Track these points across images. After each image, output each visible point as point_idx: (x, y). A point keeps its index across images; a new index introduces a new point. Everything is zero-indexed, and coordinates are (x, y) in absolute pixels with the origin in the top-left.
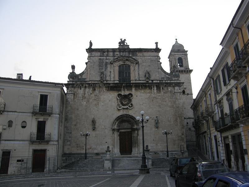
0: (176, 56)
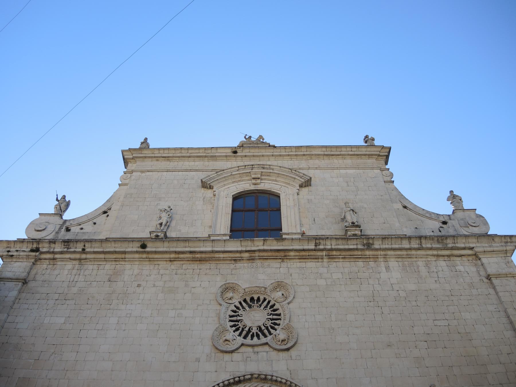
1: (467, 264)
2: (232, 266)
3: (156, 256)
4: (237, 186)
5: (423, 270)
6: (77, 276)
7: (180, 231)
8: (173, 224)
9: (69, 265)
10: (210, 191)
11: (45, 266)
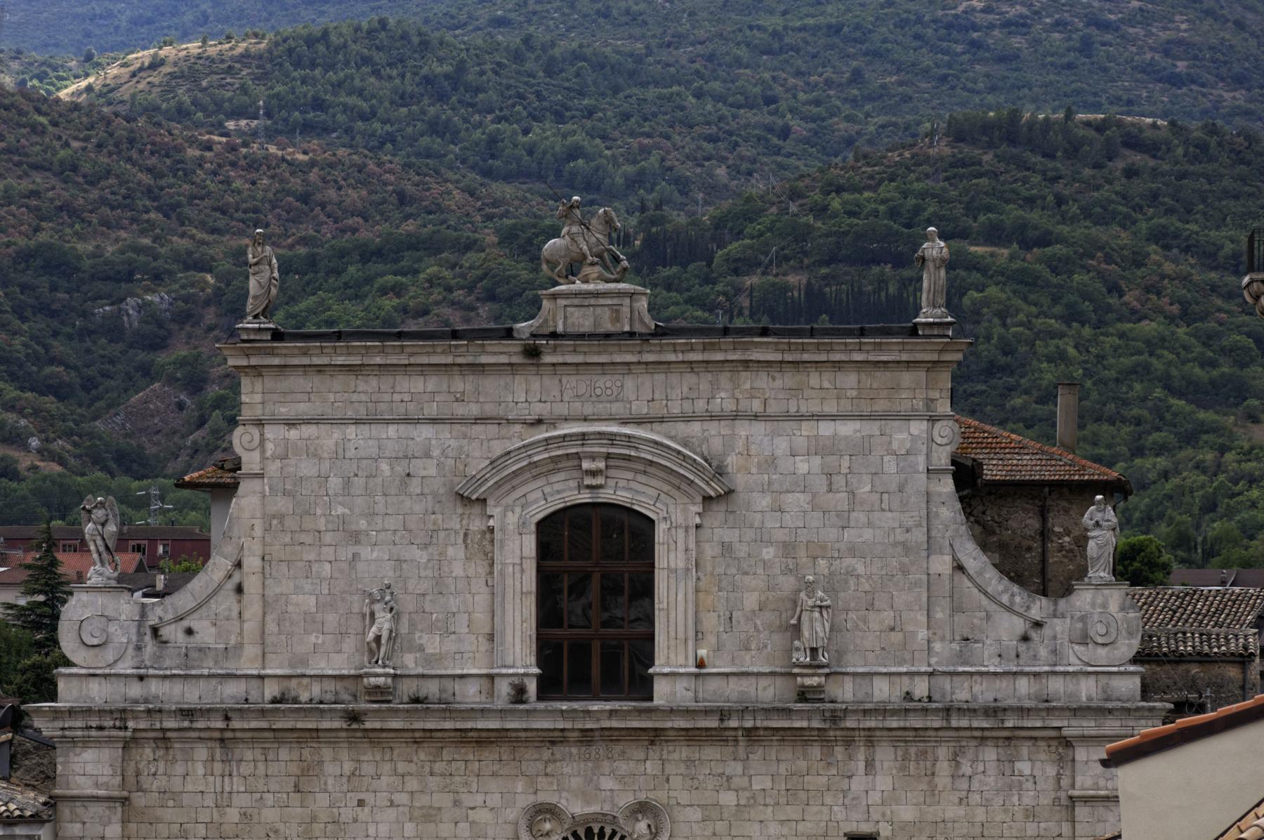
1: (1043, 756)
2: (546, 754)
3: (384, 735)
4: (547, 490)
5: (944, 767)
6: (226, 779)
7: (421, 649)
8: (404, 629)
9: (201, 753)
10: (477, 509)
11: (148, 751)
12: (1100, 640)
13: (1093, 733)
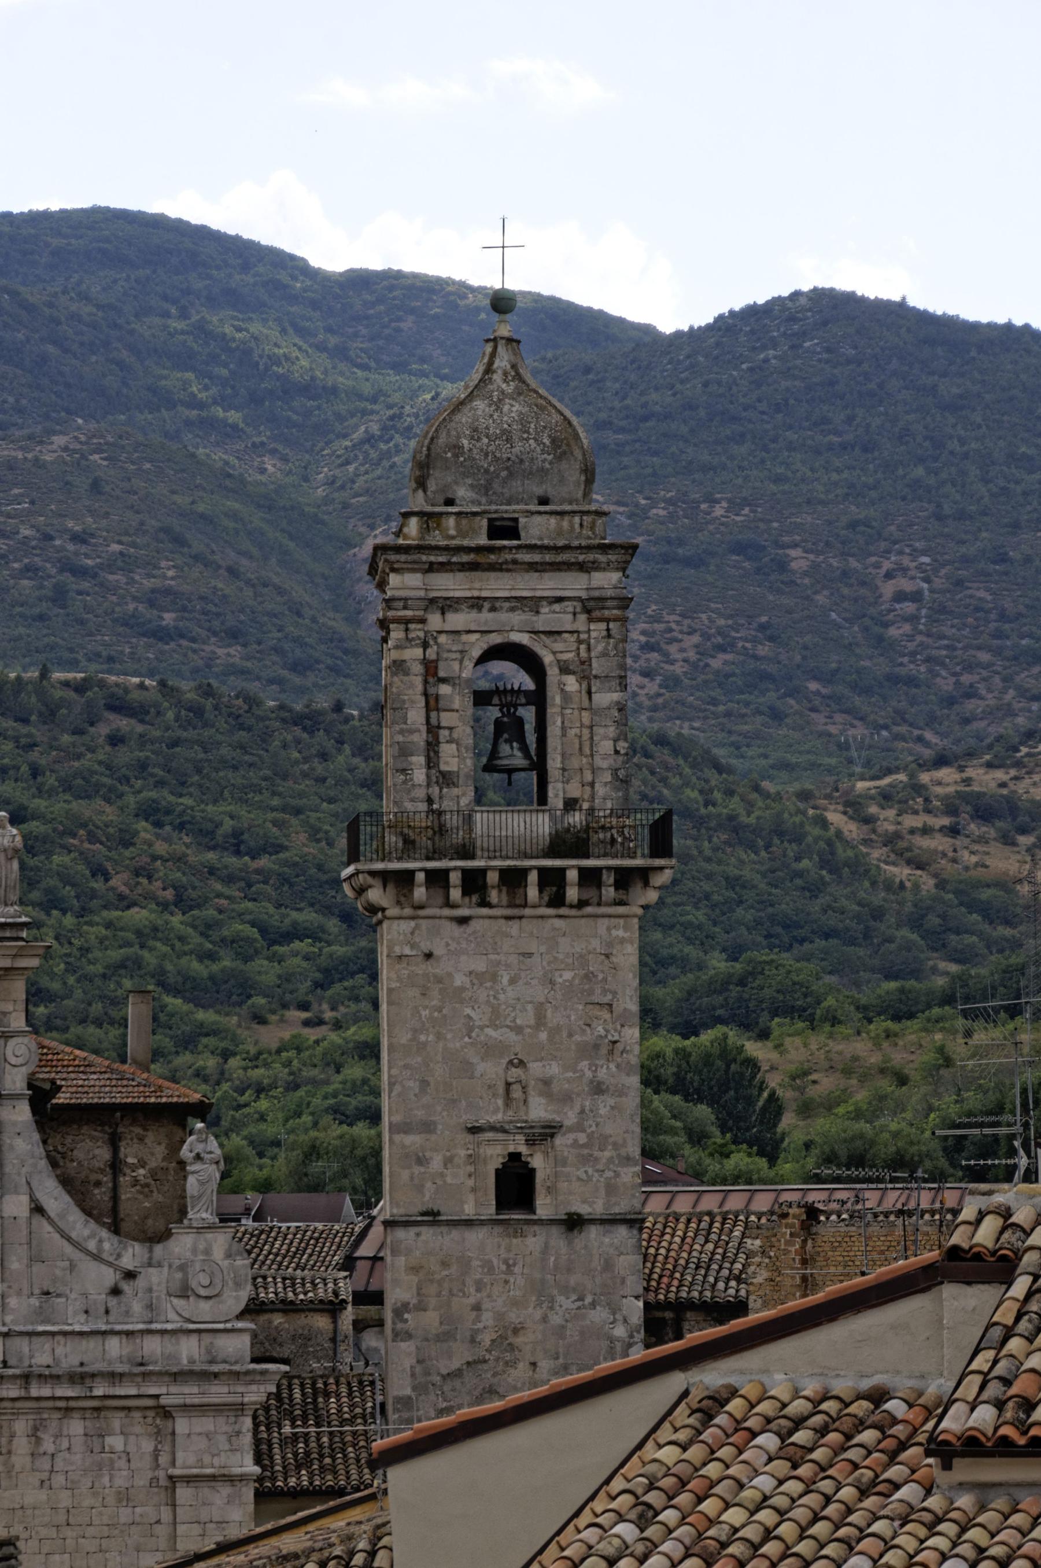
0: (457, 620)
1: (138, 1429)
5: (22, 1445)
12: (203, 1292)
13: (196, 1401)
